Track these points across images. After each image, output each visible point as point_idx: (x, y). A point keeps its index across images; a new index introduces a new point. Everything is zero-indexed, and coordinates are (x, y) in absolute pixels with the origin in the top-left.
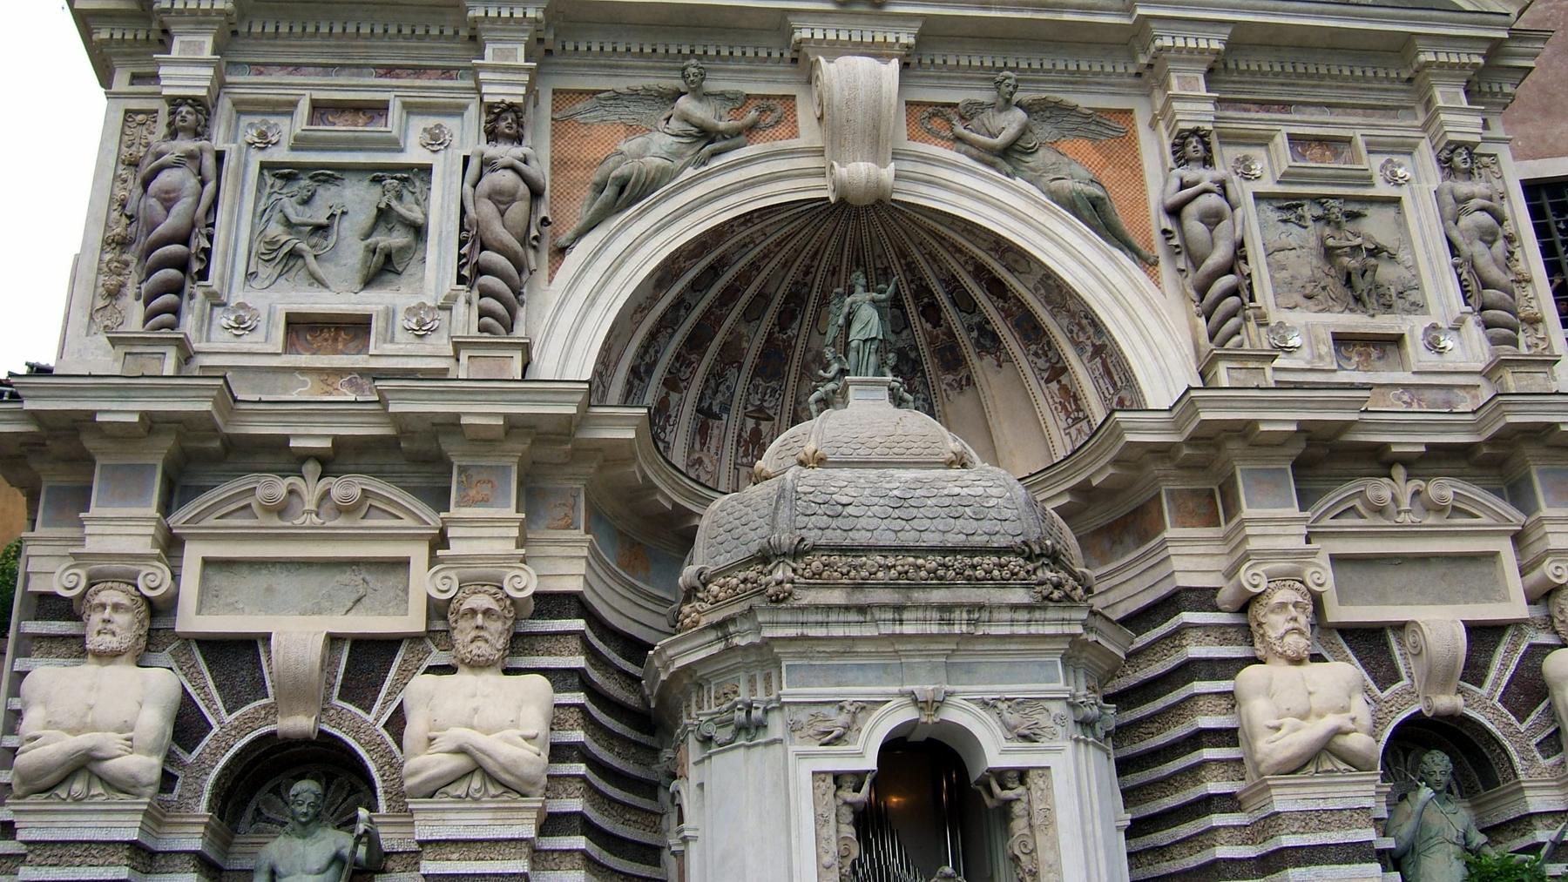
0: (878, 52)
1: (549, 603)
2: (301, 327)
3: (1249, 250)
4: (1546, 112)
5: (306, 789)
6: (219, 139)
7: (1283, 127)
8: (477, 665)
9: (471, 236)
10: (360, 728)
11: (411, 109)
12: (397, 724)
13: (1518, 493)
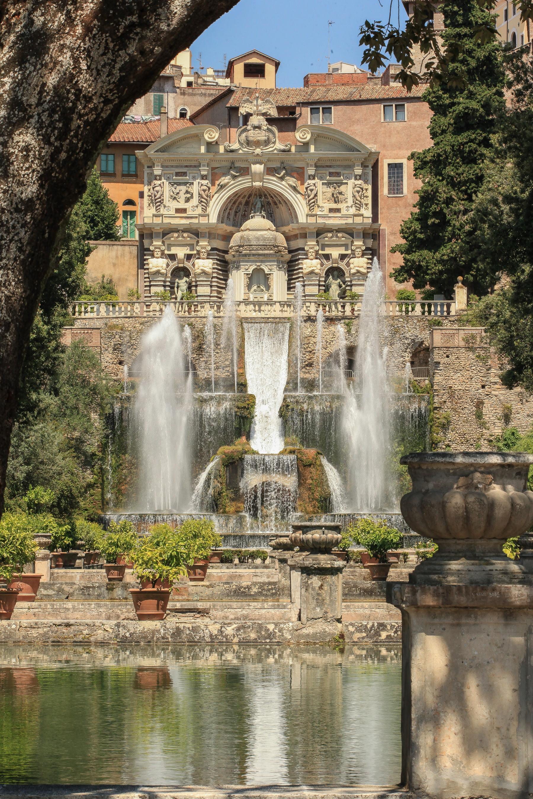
0: (261, 163)
2: (178, 211)
4: (400, 148)
8: (203, 259)
9: (200, 196)
12: (193, 265)
13: (352, 235)
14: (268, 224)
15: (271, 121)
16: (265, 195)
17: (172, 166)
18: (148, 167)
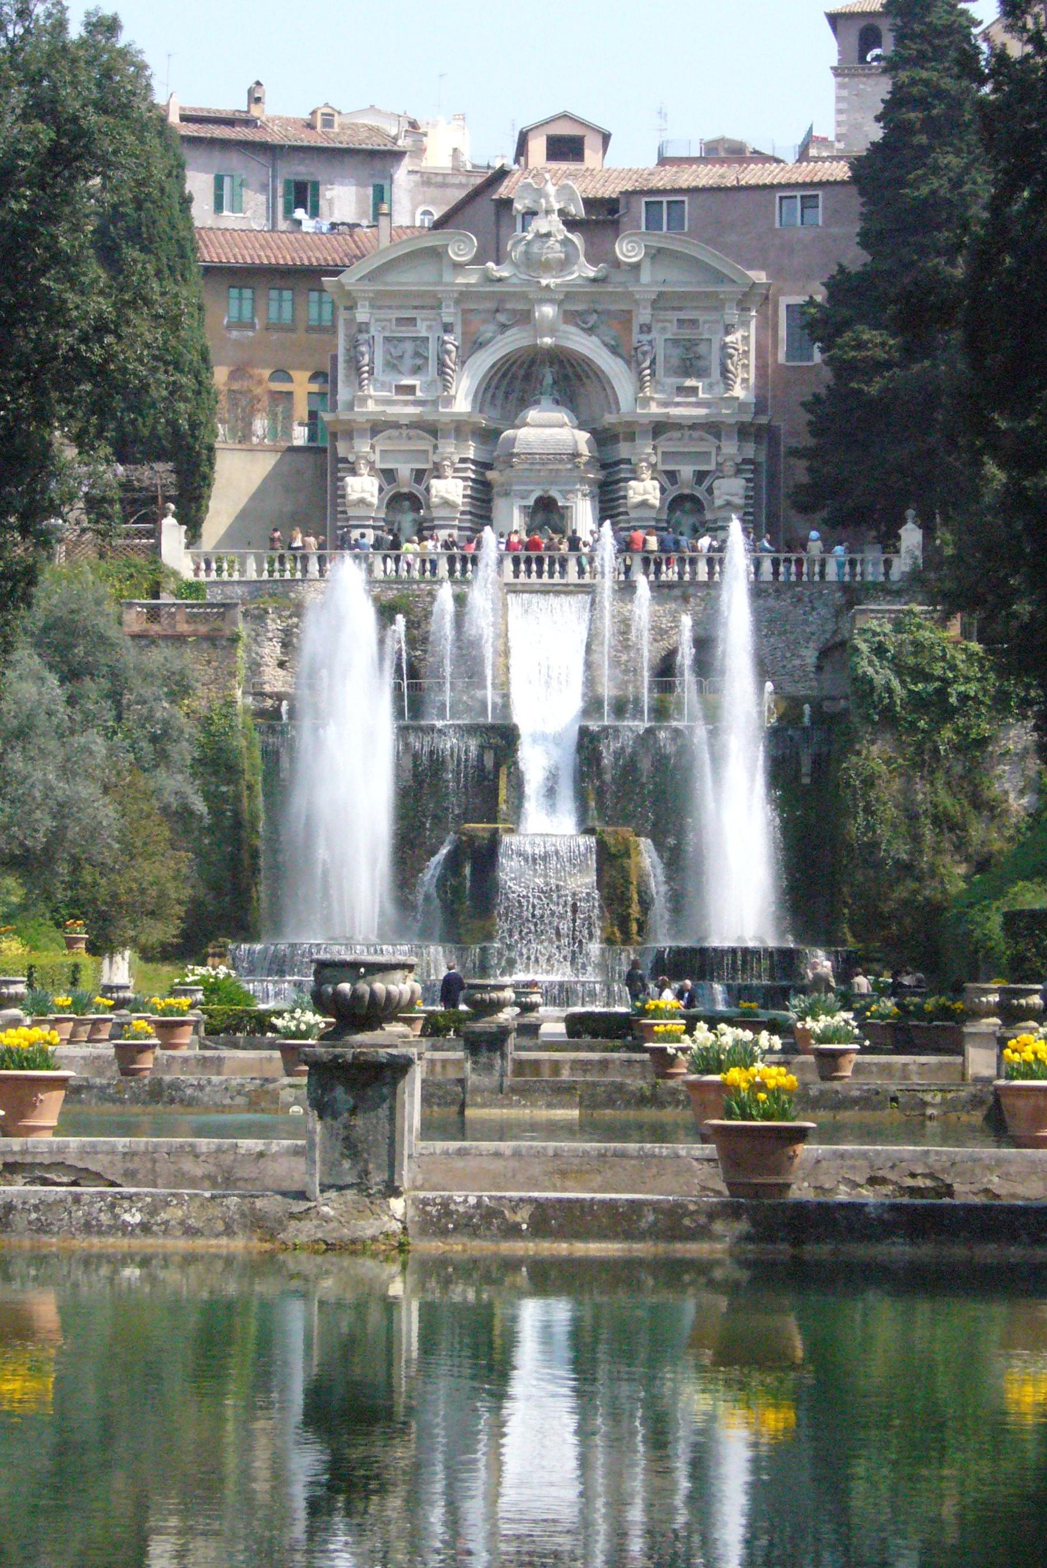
0: (551, 301)
1: (463, 460)
5: (407, 503)
6: (373, 331)
10: (418, 490)
11: (423, 320)
12: (428, 490)
13: (718, 437)
14: (562, 415)
15: (571, 224)
16: (561, 362)
17: (390, 307)
18: (346, 308)
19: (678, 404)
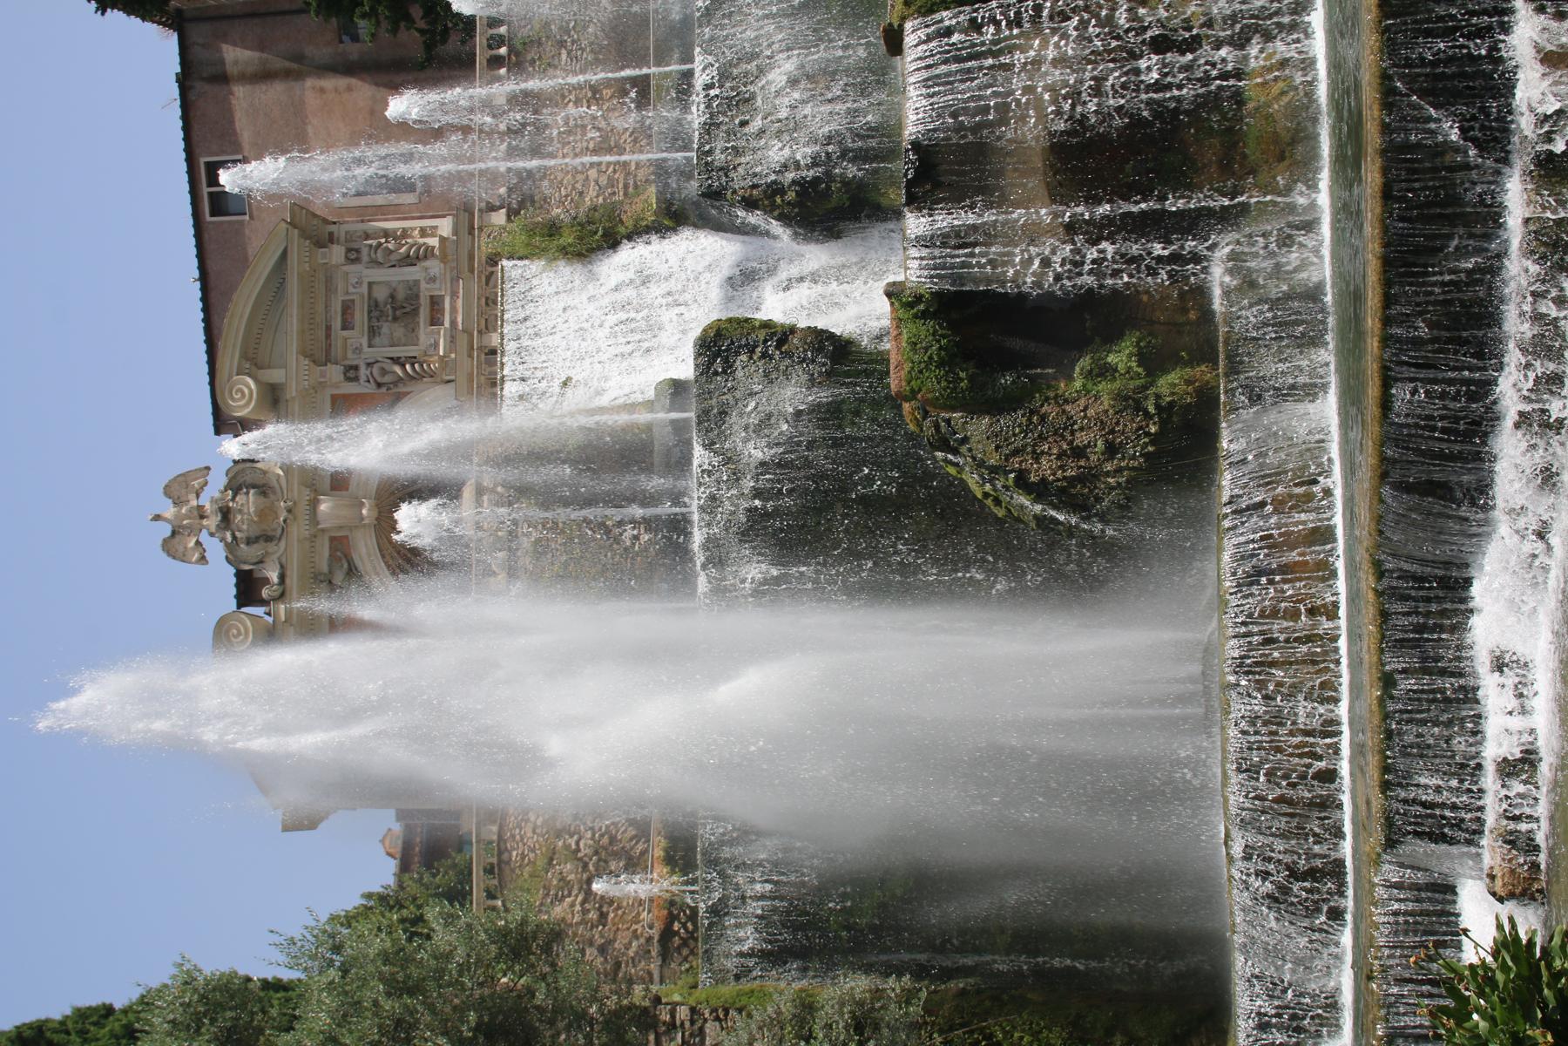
0: (314, 503)
3: (395, 355)
7: (339, 334)
19: (453, 323)
